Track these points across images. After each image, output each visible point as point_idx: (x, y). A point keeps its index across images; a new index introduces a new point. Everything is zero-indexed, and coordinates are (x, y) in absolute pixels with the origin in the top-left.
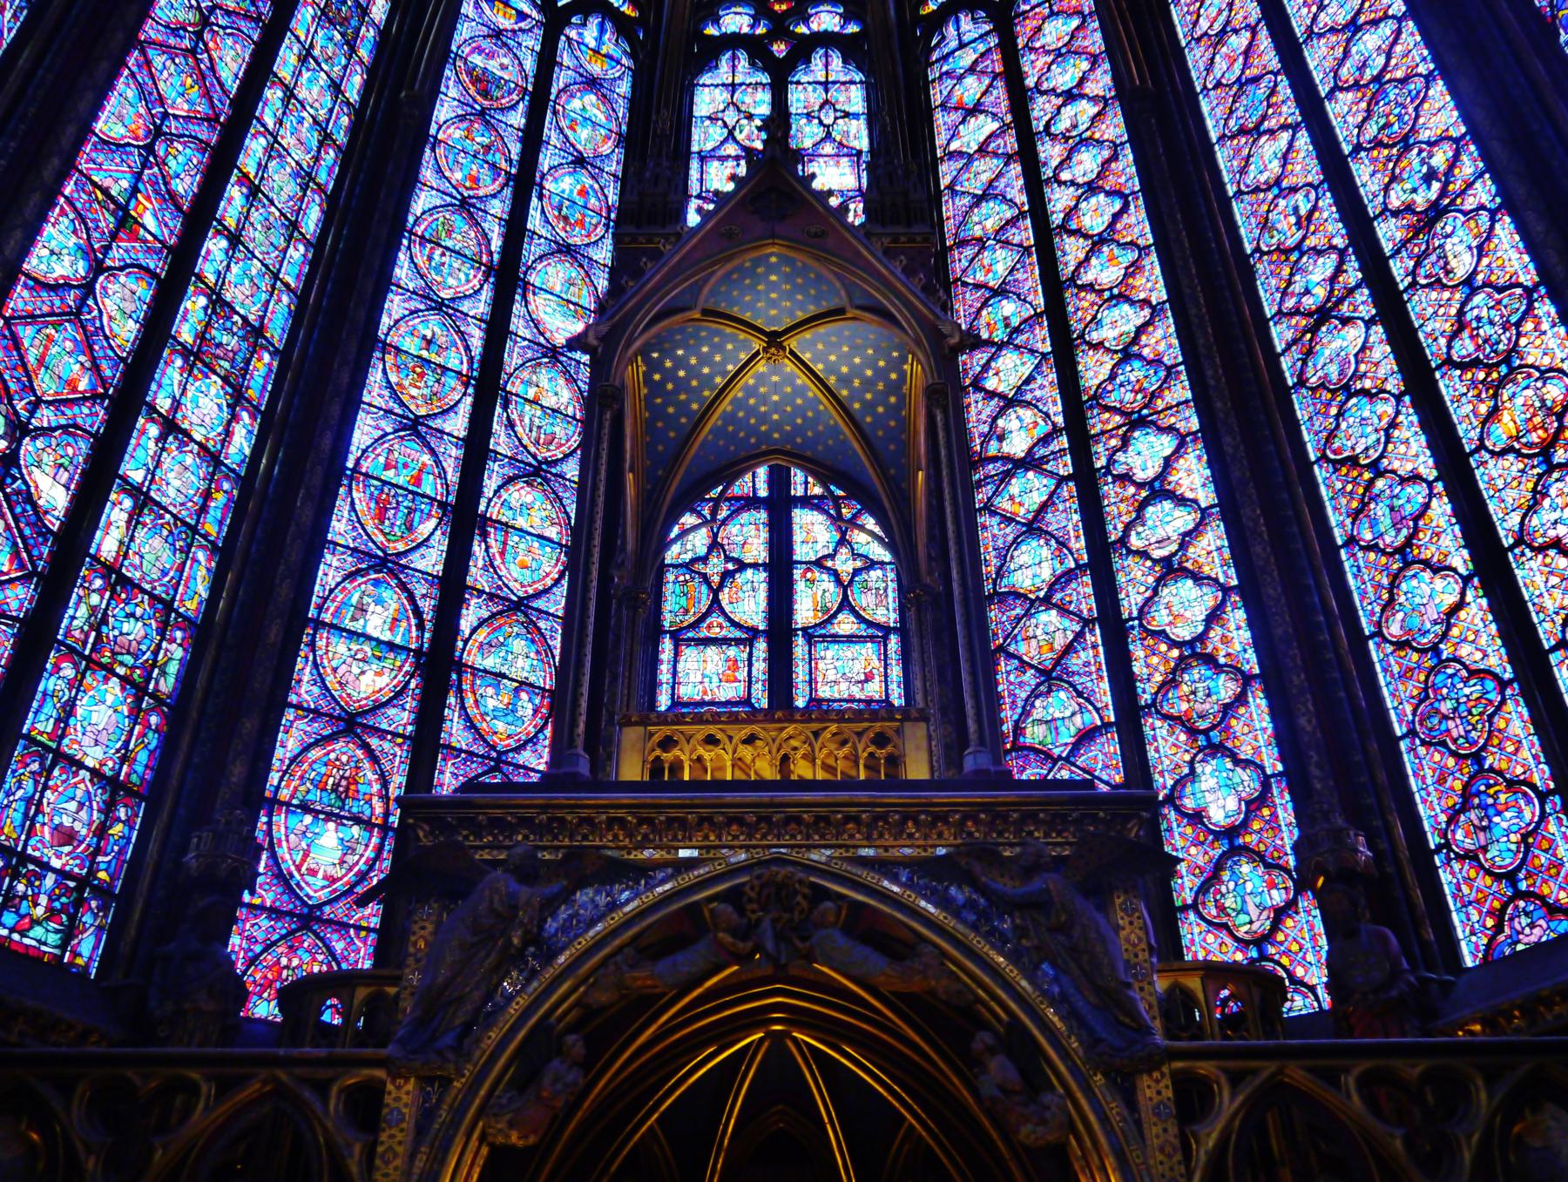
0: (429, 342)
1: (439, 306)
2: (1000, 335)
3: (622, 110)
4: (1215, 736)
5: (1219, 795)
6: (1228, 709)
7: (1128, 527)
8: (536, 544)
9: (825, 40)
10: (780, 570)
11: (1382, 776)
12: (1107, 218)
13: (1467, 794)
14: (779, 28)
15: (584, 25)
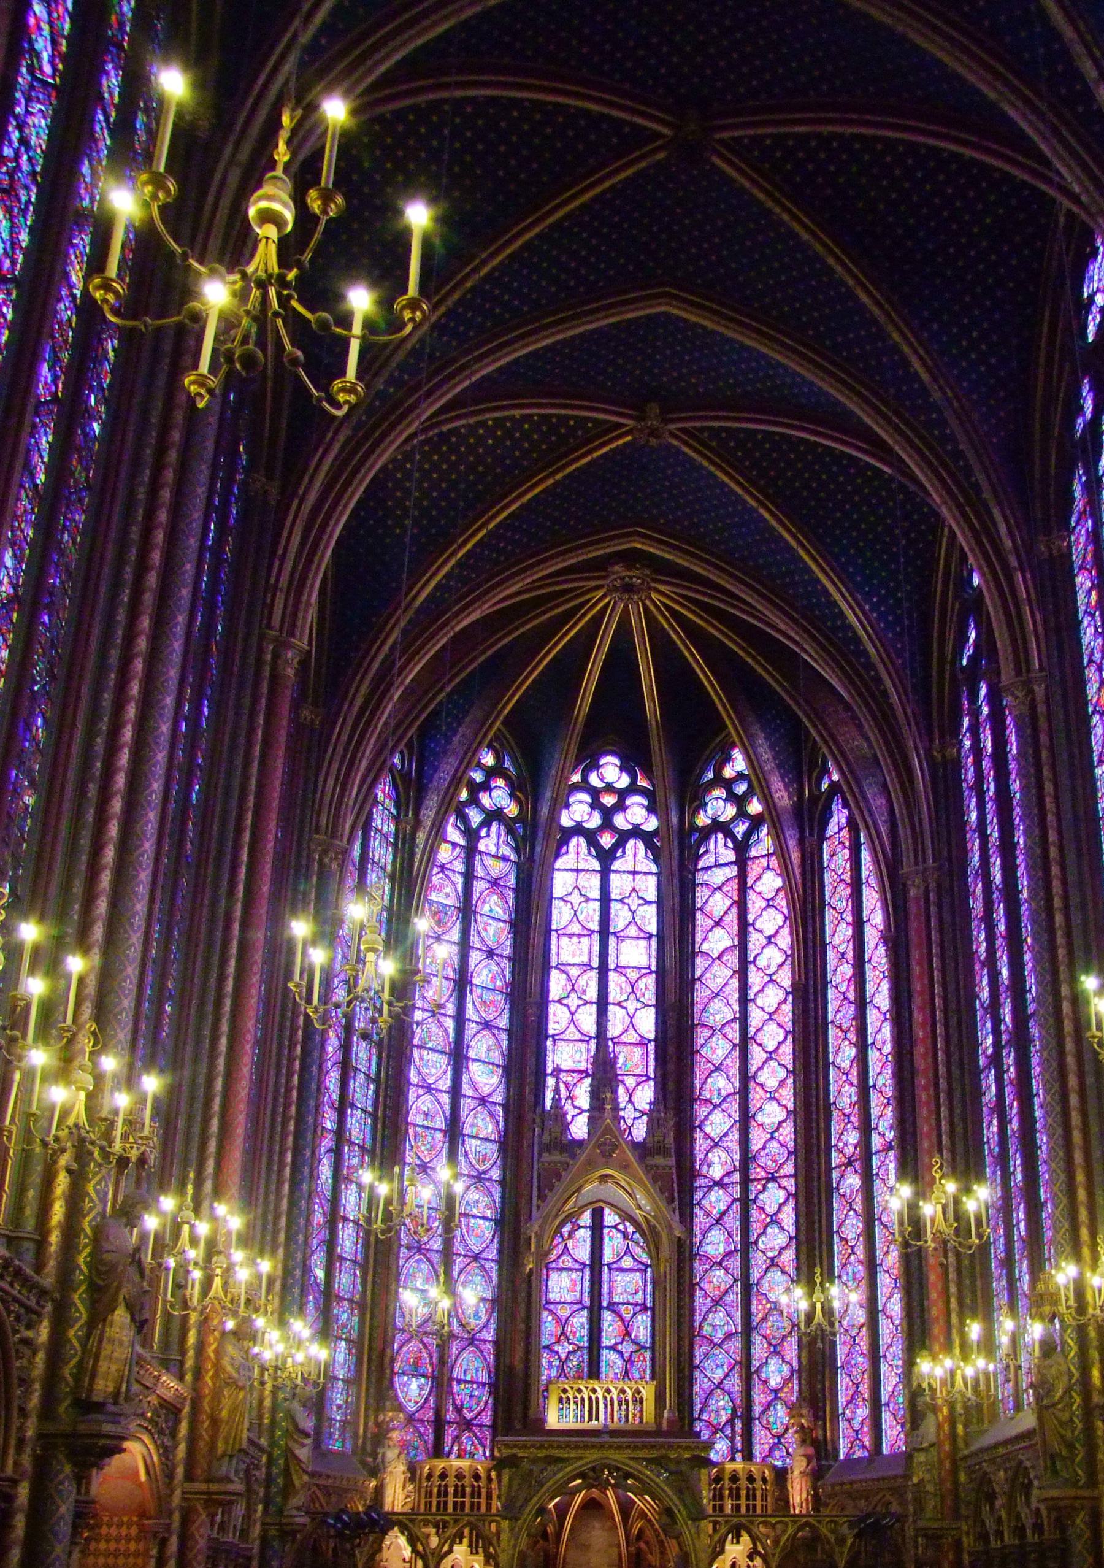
0: (426, 1115)
1: (429, 1089)
2: (716, 1100)
3: (511, 896)
4: (779, 1348)
5: (775, 1373)
6: (784, 1337)
7: (759, 1236)
8: (481, 1222)
9: (636, 832)
10: (597, 1227)
11: (827, 1384)
12: (775, 1044)
13: (852, 1398)
14: (607, 814)
15: (488, 835)
